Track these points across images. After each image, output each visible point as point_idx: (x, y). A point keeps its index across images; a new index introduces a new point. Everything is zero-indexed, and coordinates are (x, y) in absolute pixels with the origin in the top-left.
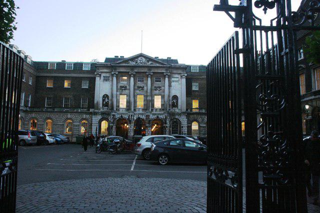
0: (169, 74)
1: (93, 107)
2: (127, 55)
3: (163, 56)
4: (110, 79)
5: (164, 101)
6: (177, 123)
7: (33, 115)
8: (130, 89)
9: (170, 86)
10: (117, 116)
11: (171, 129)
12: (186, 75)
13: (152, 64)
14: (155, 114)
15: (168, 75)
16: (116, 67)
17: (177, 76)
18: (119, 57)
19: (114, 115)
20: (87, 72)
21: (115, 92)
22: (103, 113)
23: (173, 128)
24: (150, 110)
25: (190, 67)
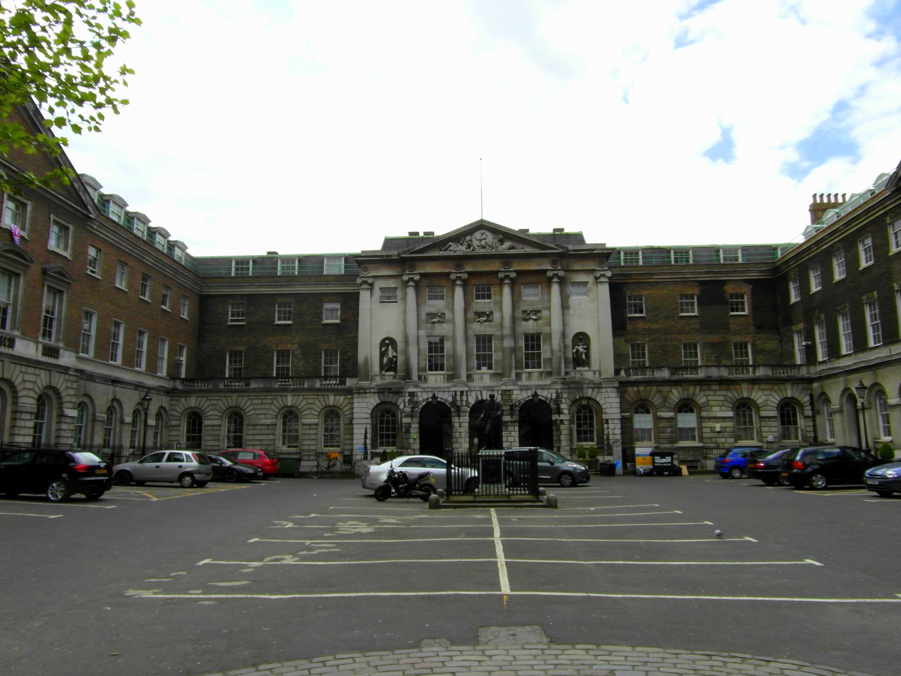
0: (561, 273)
1: (354, 376)
2: (441, 230)
3: (540, 224)
4: (399, 294)
5: (552, 352)
6: (591, 412)
7: (193, 402)
8: (453, 321)
9: (565, 306)
10: (423, 397)
11: (574, 427)
12: (609, 274)
13: (512, 248)
14: (527, 388)
15: (559, 278)
16: (413, 261)
17: (581, 278)
18: (421, 234)
19: (412, 394)
20: (338, 279)
21: (412, 331)
22: (381, 391)
23: (579, 425)
24: (513, 376)
25: (615, 252)
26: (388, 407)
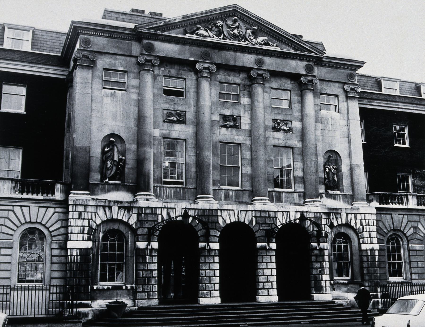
13: (267, 44)
18: (147, 13)
26: (116, 227)
